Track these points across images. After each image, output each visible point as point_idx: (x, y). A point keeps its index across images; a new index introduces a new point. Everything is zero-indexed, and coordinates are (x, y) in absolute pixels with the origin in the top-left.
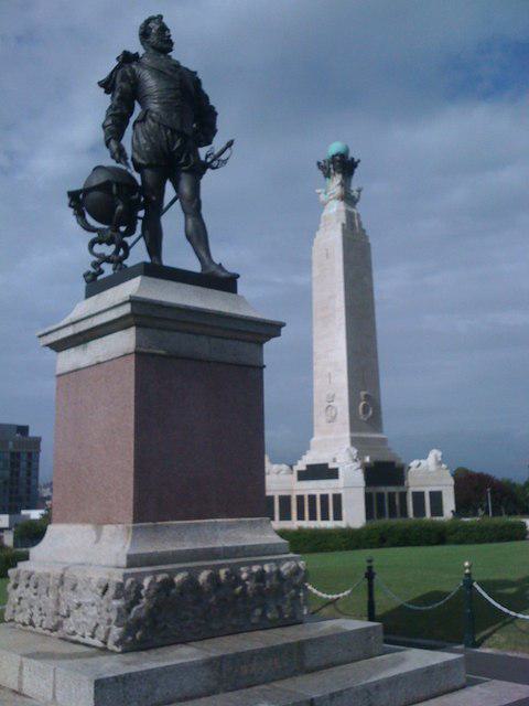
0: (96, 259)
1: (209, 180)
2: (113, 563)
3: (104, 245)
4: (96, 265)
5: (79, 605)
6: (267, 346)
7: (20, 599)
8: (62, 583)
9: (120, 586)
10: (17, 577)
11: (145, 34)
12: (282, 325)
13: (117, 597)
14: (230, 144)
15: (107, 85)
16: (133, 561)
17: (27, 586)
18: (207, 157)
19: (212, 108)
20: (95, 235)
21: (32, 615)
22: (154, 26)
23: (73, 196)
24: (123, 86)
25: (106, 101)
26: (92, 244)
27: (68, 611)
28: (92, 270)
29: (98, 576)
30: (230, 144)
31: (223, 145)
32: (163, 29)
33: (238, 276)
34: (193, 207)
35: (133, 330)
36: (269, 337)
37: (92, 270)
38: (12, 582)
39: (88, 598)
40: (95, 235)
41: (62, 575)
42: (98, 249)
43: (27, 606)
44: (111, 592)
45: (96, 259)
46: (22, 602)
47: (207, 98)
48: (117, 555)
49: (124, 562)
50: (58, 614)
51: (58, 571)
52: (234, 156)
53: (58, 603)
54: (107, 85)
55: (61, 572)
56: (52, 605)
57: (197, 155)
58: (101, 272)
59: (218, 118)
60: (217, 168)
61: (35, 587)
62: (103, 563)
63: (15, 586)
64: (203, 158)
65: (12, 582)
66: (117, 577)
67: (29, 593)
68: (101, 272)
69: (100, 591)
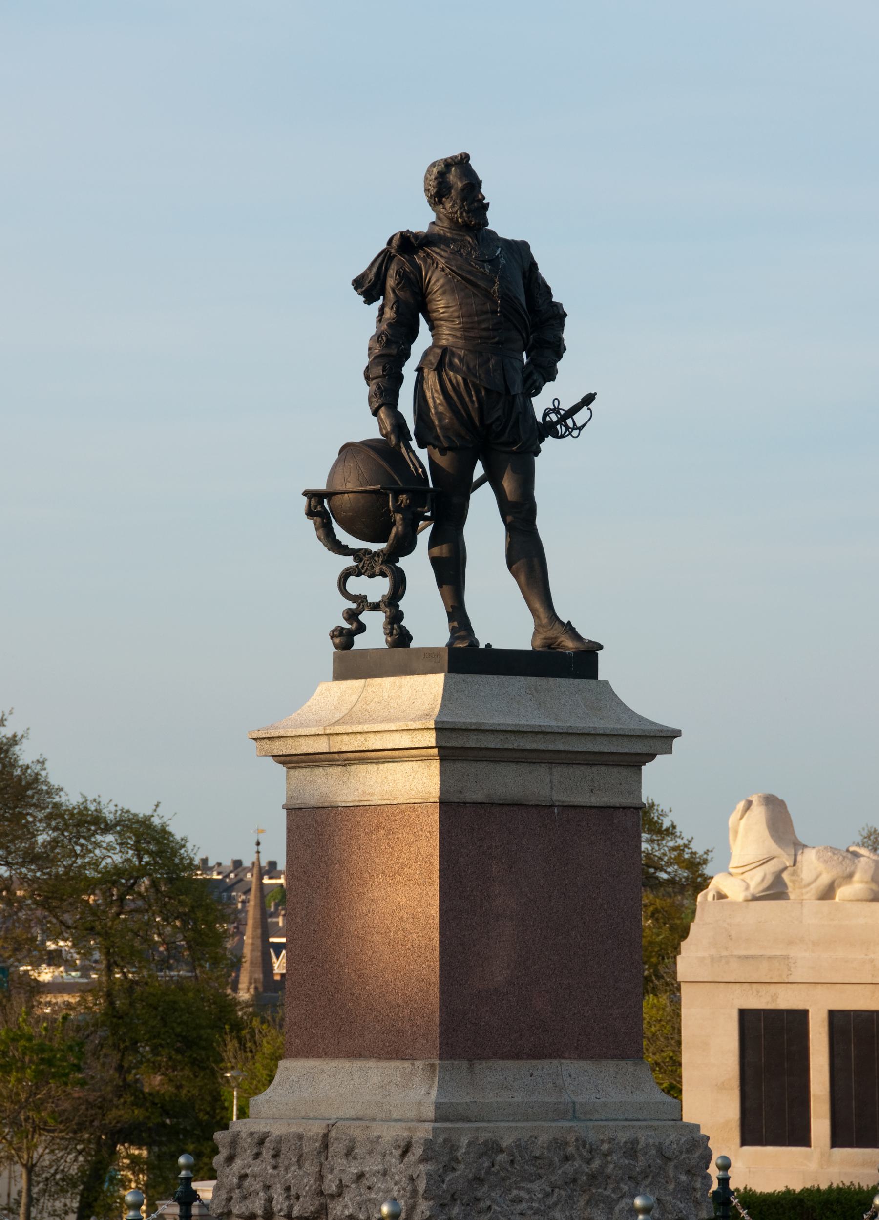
0: (354, 606)
1: (552, 459)
2: (412, 1114)
3: (364, 578)
4: (352, 616)
5: (360, 1176)
6: (647, 769)
7: (243, 1177)
8: (326, 1146)
9: (429, 1144)
10: (234, 1143)
11: (439, 193)
12: (677, 734)
13: (424, 1159)
14: (589, 399)
15: (369, 287)
16: (443, 1114)
17: (257, 1156)
18: (545, 415)
19: (558, 306)
20: (349, 562)
21: (270, 1200)
22: (453, 177)
23: (314, 497)
24: (397, 279)
25: (365, 320)
26: (344, 577)
27: (341, 1186)
28: (346, 625)
29: (390, 1133)
30: (589, 399)
31: (578, 400)
32: (473, 184)
33: (601, 647)
34: (520, 517)
35: (435, 765)
36: (651, 757)
37: (346, 625)
38: (224, 1153)
39: (372, 1165)
40: (349, 562)
41: (326, 1136)
42: (355, 585)
43: (258, 1186)
44: (418, 1151)
45: (354, 606)
46: (246, 1183)
47: (548, 290)
48: (419, 1104)
49: (429, 1112)
50: (321, 1193)
51: (317, 1129)
52: (598, 421)
53: (321, 1177)
54: (369, 287)
55: (322, 1131)
56: (310, 1182)
57: (528, 410)
58: (361, 628)
59: (567, 321)
60: (562, 436)
61: (275, 1156)
62: (395, 1116)
63: (230, 1159)
64: (539, 419)
65: (224, 1153)
66: (424, 1132)
67: (264, 1166)
68: (361, 628)
69: (397, 1153)
